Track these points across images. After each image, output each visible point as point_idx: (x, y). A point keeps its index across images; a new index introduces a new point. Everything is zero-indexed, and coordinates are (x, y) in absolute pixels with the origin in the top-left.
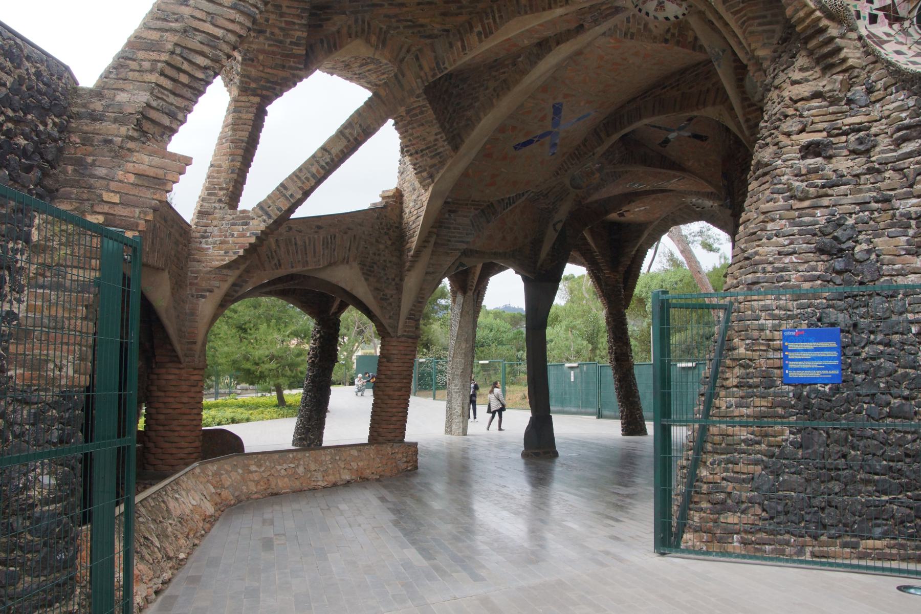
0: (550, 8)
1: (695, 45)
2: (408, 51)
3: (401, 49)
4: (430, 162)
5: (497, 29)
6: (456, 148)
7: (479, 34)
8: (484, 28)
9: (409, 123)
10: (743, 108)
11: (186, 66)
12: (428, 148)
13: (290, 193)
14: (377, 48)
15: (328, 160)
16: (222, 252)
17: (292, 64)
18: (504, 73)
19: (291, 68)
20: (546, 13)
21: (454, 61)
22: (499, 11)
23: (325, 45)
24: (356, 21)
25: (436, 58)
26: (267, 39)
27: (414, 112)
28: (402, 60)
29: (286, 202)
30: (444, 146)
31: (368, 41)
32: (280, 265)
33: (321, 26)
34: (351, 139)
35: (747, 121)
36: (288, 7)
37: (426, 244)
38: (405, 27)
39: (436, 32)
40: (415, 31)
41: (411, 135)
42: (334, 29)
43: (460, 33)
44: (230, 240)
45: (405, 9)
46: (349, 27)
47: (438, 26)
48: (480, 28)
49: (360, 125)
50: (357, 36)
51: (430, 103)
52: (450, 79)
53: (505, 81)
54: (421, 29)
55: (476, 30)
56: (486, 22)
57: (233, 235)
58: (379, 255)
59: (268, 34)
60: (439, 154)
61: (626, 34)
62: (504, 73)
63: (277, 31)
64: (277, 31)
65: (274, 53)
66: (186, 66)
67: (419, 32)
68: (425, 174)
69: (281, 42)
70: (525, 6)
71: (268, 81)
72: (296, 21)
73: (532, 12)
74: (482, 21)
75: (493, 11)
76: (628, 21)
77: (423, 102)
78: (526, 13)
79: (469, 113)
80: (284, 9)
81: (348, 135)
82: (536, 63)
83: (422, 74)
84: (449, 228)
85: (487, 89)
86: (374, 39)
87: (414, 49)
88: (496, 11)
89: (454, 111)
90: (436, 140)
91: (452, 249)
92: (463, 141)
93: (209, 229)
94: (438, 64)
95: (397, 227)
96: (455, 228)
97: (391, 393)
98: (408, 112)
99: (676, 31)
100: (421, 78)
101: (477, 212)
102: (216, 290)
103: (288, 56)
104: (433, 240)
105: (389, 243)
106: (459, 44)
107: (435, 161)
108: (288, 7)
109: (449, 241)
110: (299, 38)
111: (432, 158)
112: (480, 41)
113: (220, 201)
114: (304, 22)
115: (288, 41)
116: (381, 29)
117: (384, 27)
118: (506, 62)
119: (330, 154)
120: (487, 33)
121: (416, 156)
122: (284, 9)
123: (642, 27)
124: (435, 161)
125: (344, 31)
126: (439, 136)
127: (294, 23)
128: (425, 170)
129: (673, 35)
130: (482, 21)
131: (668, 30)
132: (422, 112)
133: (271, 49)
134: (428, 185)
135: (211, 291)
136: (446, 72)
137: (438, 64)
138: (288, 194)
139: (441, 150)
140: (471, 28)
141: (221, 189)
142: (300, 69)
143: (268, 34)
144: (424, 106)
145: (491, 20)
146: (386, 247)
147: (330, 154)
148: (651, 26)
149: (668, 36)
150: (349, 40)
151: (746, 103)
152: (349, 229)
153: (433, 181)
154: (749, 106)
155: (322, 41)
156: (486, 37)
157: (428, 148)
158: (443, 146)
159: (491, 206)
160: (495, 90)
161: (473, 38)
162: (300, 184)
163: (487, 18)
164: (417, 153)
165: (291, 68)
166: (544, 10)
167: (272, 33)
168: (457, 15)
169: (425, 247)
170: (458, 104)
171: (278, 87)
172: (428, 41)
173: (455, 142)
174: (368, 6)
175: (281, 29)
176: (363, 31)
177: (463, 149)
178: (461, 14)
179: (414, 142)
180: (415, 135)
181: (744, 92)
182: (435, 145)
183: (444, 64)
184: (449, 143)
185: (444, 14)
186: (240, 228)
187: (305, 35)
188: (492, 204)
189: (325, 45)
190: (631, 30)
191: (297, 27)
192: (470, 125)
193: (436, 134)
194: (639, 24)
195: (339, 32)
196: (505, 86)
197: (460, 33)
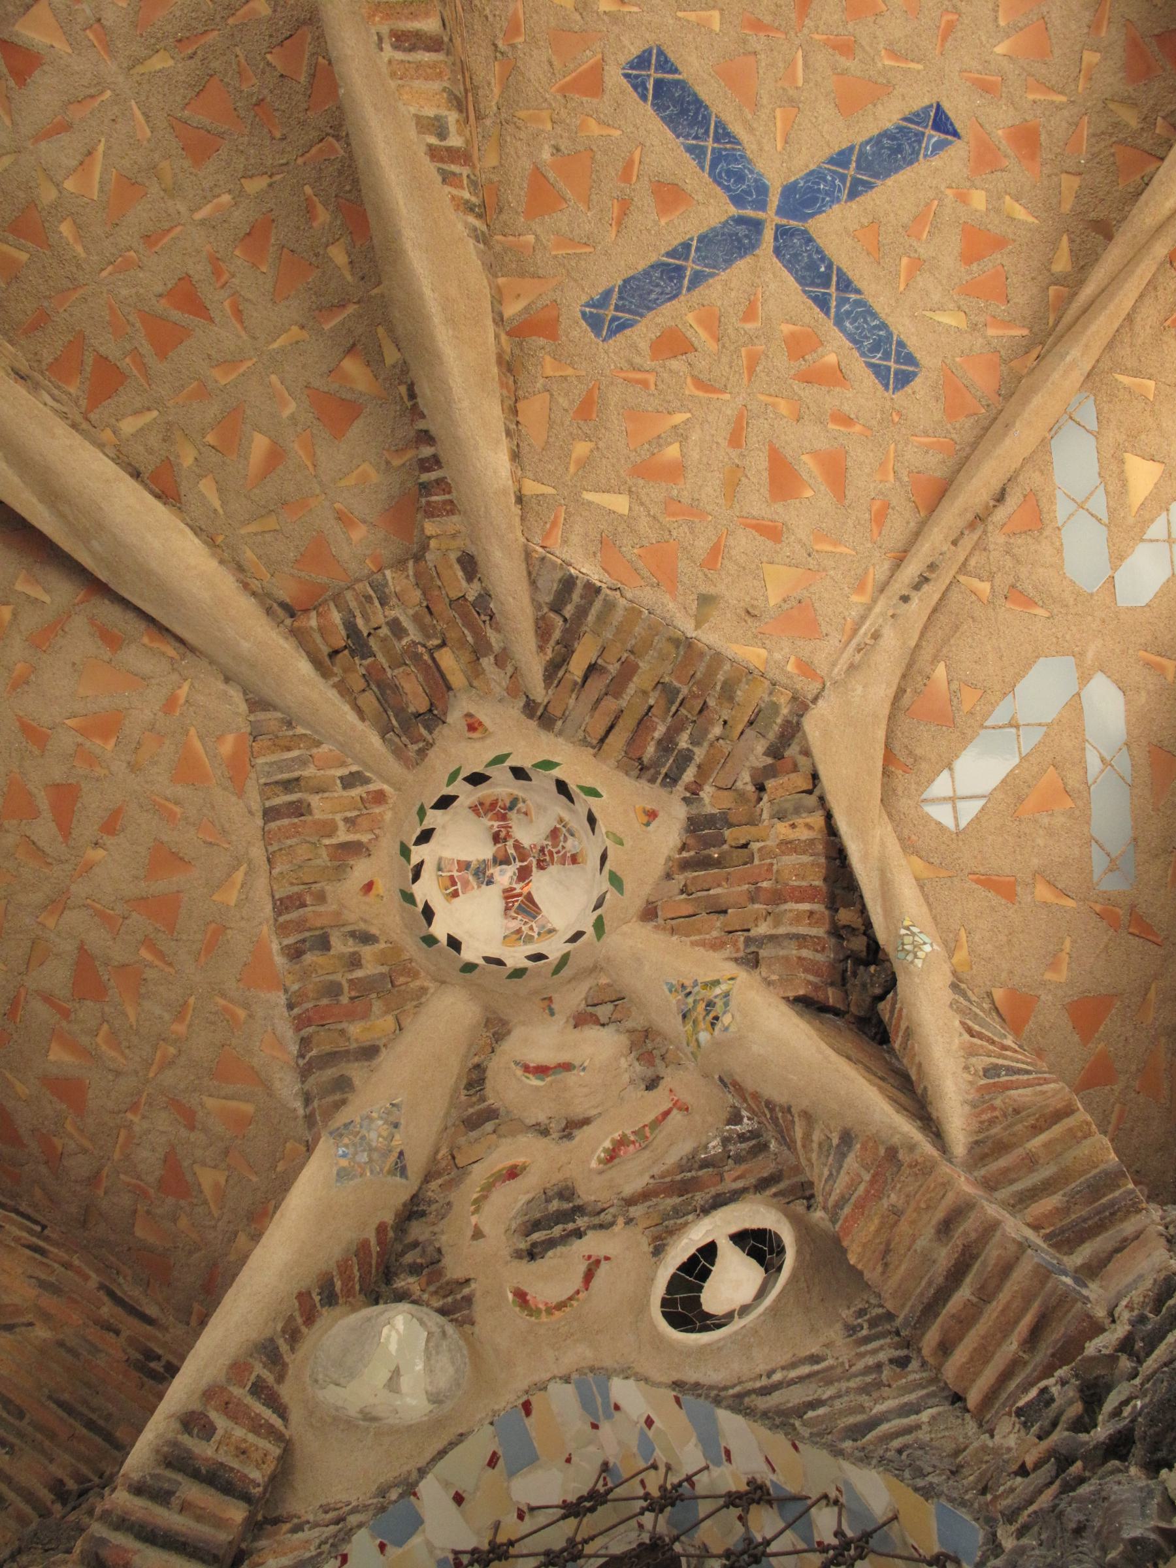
1: (330, 1071)
10: (237, 1369)
35: (193, 1422)
61: (288, 785)
76: (349, 781)
99: (371, 968)
123: (343, 836)
129: (355, 962)
131: (367, 938)
148: (361, 870)
149: (341, 946)
151: (259, 1370)
154: (258, 1389)
181: (294, 1336)
190: (315, 800)
194: (351, 822)
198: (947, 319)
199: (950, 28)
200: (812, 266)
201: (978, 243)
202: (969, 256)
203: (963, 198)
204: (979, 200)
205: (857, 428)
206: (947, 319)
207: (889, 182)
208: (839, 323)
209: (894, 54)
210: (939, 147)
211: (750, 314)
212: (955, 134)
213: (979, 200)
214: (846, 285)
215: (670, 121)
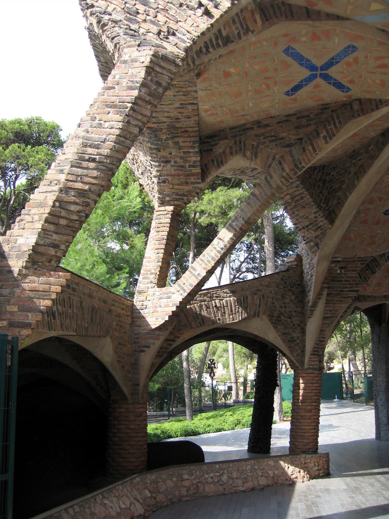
0: (378, 108)
2: (274, 159)
3: (268, 157)
4: (314, 234)
5: (338, 132)
6: (332, 222)
7: (325, 137)
8: (327, 132)
9: (294, 207)
11: (63, 213)
12: (311, 224)
13: (197, 273)
14: (251, 160)
15: (222, 246)
16: (154, 319)
17: (192, 180)
18: (360, 160)
19: (192, 183)
20: (374, 113)
21: (309, 160)
22: (338, 118)
23: (215, 163)
24: (235, 143)
25: (294, 160)
26: (172, 166)
27: (297, 198)
28: (270, 166)
29: (195, 280)
30: (322, 221)
31: (245, 156)
32: (204, 323)
33: (211, 150)
34: (238, 229)
36: (183, 142)
37: (320, 296)
38: (270, 142)
39: (293, 141)
40: (278, 142)
41: (298, 215)
42: (221, 151)
43: (310, 140)
44: (159, 309)
45: (268, 129)
46: (231, 147)
47: (294, 137)
48: (325, 133)
49: (243, 218)
50: (236, 153)
51: (307, 190)
52: (323, 169)
53: (361, 166)
54: (282, 141)
55: (322, 135)
56: (329, 128)
57: (161, 306)
58: (285, 307)
59: (172, 163)
60: (320, 227)
62: (360, 160)
63: (178, 160)
64: (178, 160)
65: (179, 175)
66: (63, 213)
67: (281, 143)
68: (312, 244)
69: (182, 167)
70: (358, 110)
71: (178, 195)
72: (190, 150)
73: (364, 114)
74: (325, 127)
75: (333, 119)
77: (301, 190)
78: (359, 116)
79: (339, 194)
80: (181, 144)
81: (235, 227)
82: (382, 149)
83: (284, 174)
84: (341, 281)
85: (349, 174)
86: (248, 153)
87: (277, 157)
88: (336, 119)
89: (329, 193)
90: (316, 217)
91: (345, 298)
92: (337, 216)
93: (145, 303)
94: (296, 165)
95: (299, 285)
96: (346, 281)
97: (303, 414)
98: (292, 199)
100: (284, 177)
101: (363, 266)
102: (152, 346)
103: (189, 175)
104: (325, 292)
105: (293, 297)
106: (310, 148)
107: (318, 233)
108: (183, 142)
109: (342, 291)
110: (195, 162)
111: (315, 231)
112: (327, 143)
113: (151, 282)
114: (196, 150)
115: (187, 165)
116: (253, 145)
117: (255, 144)
118: (361, 152)
119: (223, 241)
120: (331, 136)
121: (303, 230)
122: (181, 144)
124: (318, 233)
125: (228, 151)
126: (317, 214)
127: (190, 152)
128: (312, 240)
130: (325, 127)
132: (302, 198)
133: (176, 172)
134: (316, 252)
135: (148, 347)
136: (304, 169)
137: (296, 165)
138: (196, 274)
139: (321, 224)
140: (318, 134)
141: (152, 274)
142: (199, 183)
143: (172, 163)
144: (303, 193)
145: (333, 126)
146: (291, 300)
147: (223, 241)
150: (231, 157)
152: (258, 290)
153: (319, 248)
155: (213, 161)
156: (331, 139)
157: (311, 224)
158: (322, 221)
159: (374, 260)
160: (355, 174)
161: (321, 142)
162: (204, 266)
163: (330, 125)
164: (304, 228)
165: (192, 183)
166: (373, 110)
167: (175, 162)
168: (307, 126)
169: (320, 299)
170: (331, 187)
171: (185, 198)
172: (287, 149)
173: (331, 217)
174: (243, 130)
175: (181, 158)
176: (241, 149)
177: (337, 222)
178: (310, 125)
179: (300, 220)
180: (301, 215)
182: (316, 221)
183: (301, 164)
184: (326, 219)
185: (297, 127)
186: (165, 300)
187: (199, 159)
188: (375, 258)
189: (215, 163)
191: (192, 154)
192: (341, 203)
193: (315, 213)
195: (224, 152)
196: (362, 171)
197: (310, 140)
198: (337, 41)
199: (264, 54)
200: (329, 64)
201: (315, 37)
202: (319, 39)
203: (304, 42)
204: (304, 39)
205: (368, 55)
206: (337, 41)
207: (305, 56)
208: (342, 59)
209: (275, 61)
210: (293, 49)
211: (343, 72)
212: (289, 46)
213: (304, 39)
214: (333, 59)
215: (300, 89)
